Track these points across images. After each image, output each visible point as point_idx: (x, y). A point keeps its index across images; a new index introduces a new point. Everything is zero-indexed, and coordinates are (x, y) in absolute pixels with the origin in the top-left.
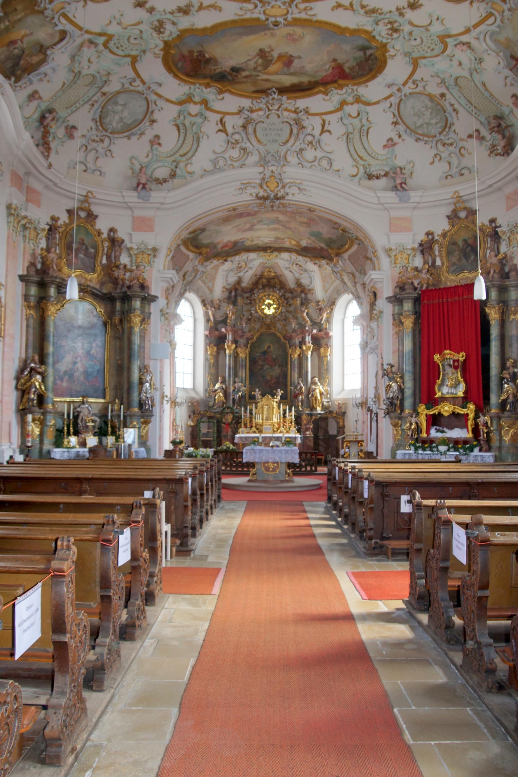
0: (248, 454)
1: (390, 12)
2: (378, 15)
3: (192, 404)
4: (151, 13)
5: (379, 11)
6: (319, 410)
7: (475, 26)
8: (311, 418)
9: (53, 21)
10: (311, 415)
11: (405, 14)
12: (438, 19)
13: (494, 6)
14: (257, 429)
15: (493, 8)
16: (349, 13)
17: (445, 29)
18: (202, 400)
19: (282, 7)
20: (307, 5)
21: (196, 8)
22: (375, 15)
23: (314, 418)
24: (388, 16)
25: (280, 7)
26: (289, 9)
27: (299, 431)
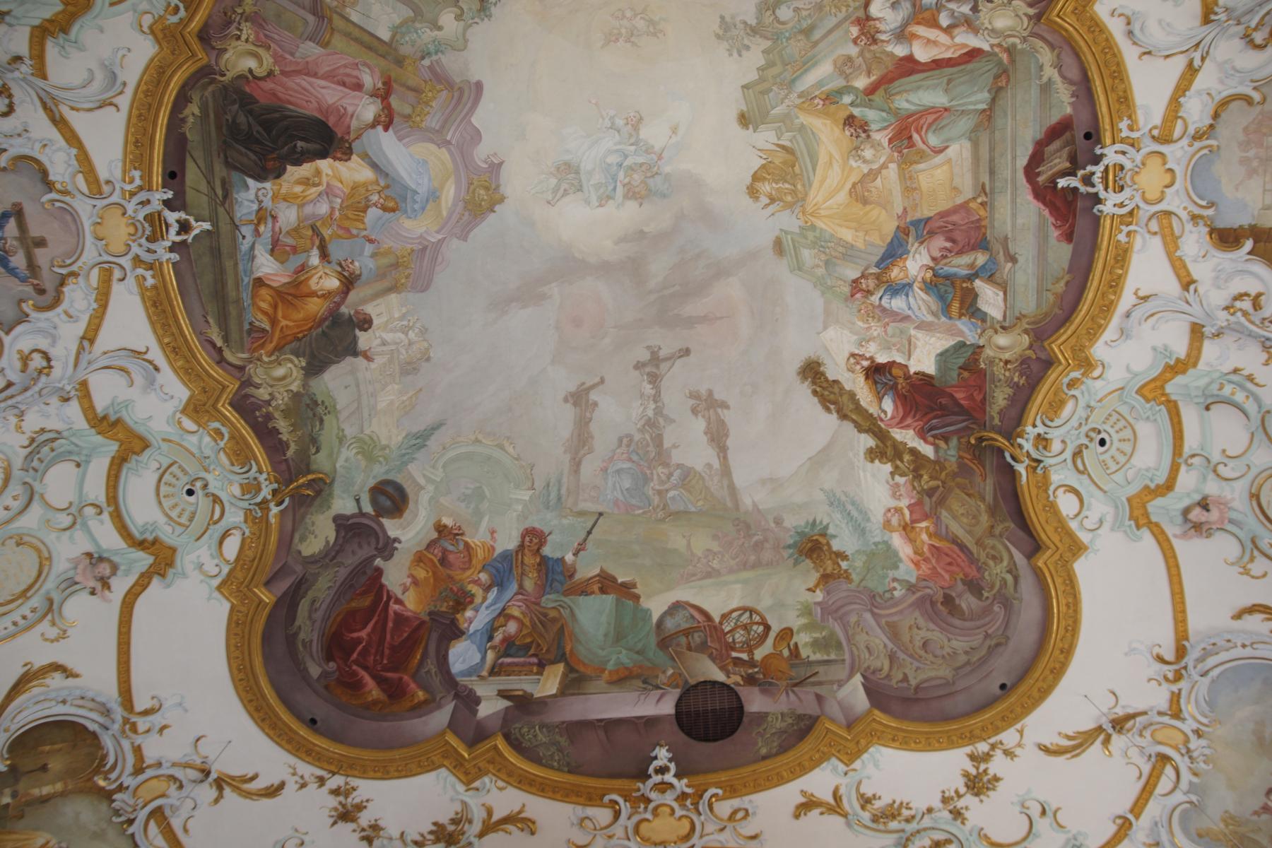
1: (930, 810)
2: (904, 825)
4: (369, 840)
5: (906, 813)
7: (1138, 807)
9: (131, 830)
11: (967, 814)
12: (1044, 812)
13: (1159, 736)
15: (1160, 743)
16: (837, 820)
17: (1068, 840)
19: (679, 812)
20: (736, 803)
21: (477, 827)
22: (894, 825)
24: (927, 822)
25: (673, 811)
26: (695, 817)
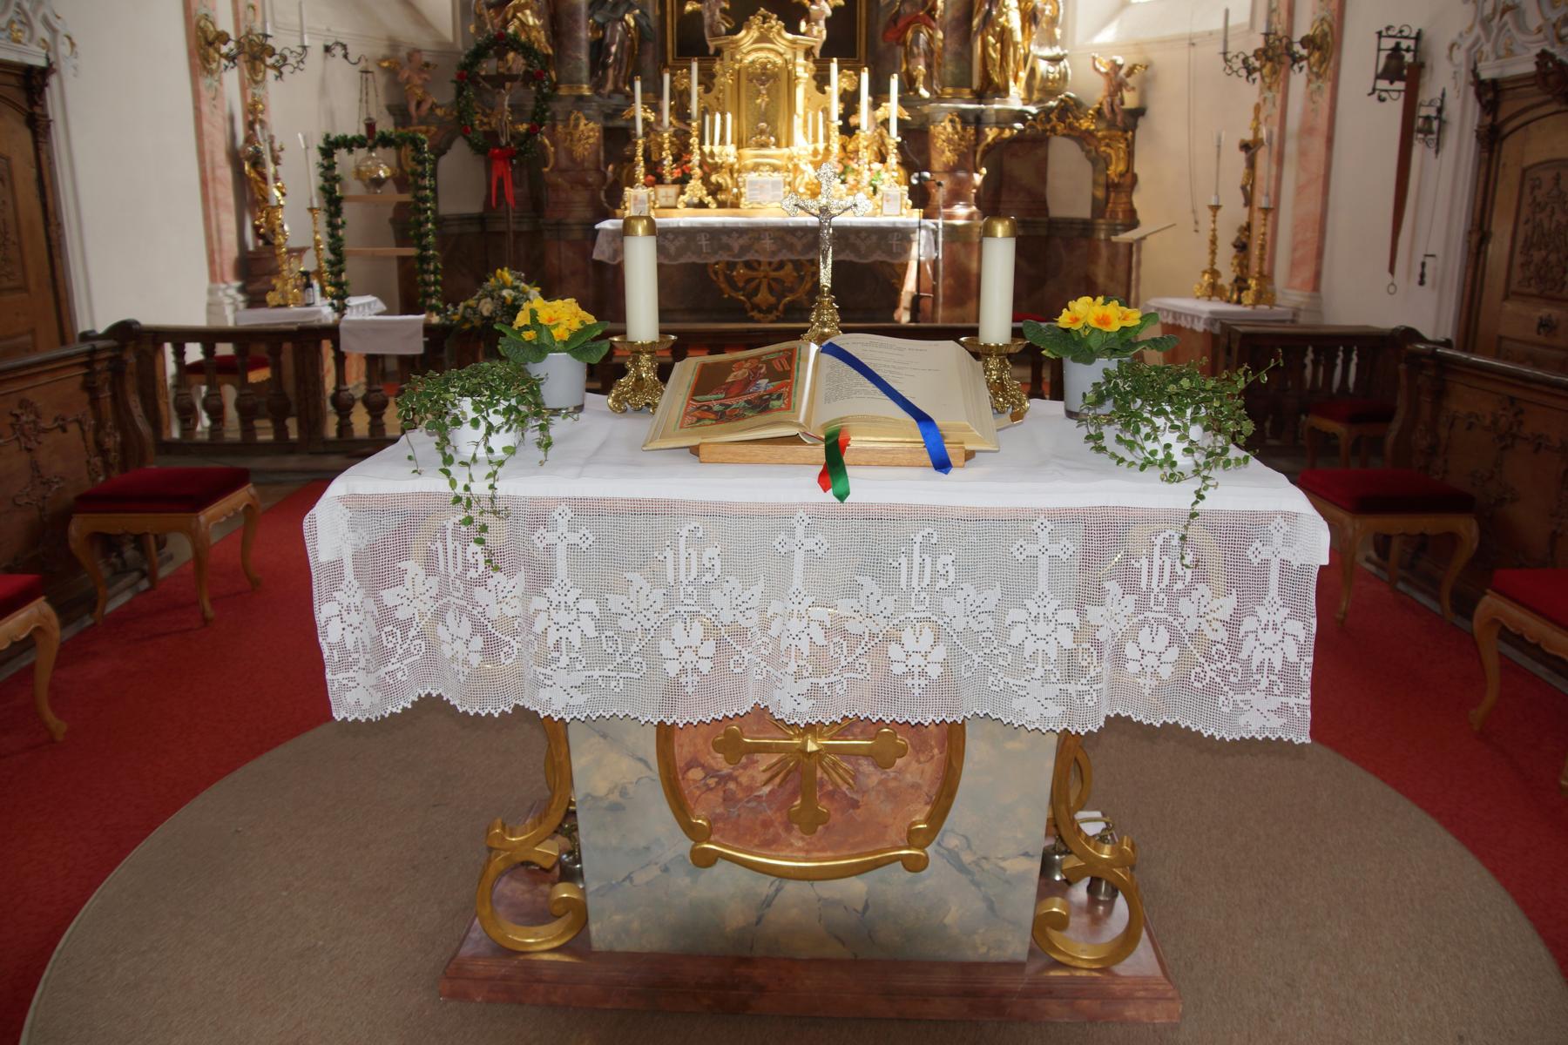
0: (413, 593)
3: (392, 72)
6: (1015, 100)
8: (979, 133)
10: (976, 121)
14: (715, 190)
18: (445, 51)
23: (991, 134)
27: (920, 197)
